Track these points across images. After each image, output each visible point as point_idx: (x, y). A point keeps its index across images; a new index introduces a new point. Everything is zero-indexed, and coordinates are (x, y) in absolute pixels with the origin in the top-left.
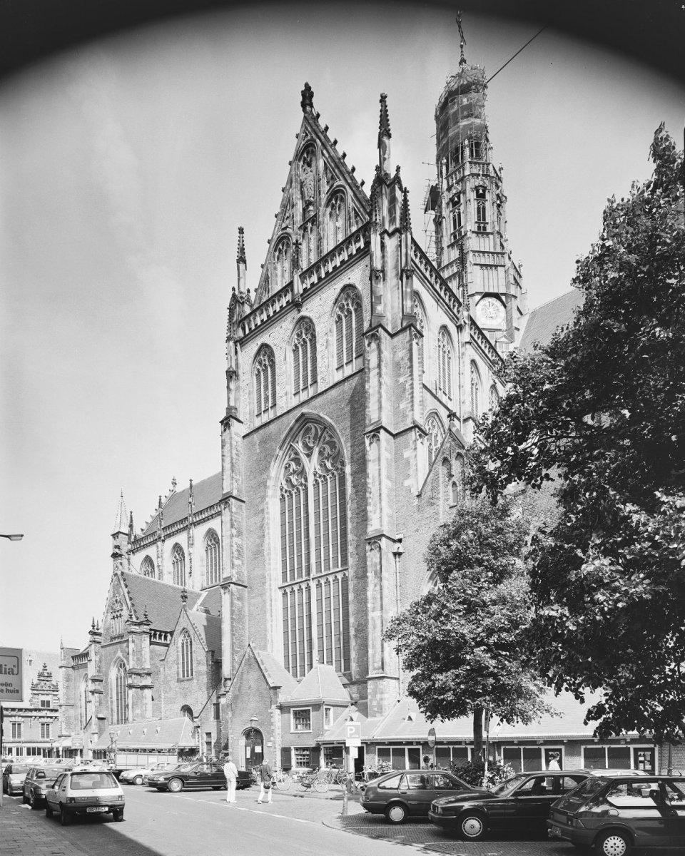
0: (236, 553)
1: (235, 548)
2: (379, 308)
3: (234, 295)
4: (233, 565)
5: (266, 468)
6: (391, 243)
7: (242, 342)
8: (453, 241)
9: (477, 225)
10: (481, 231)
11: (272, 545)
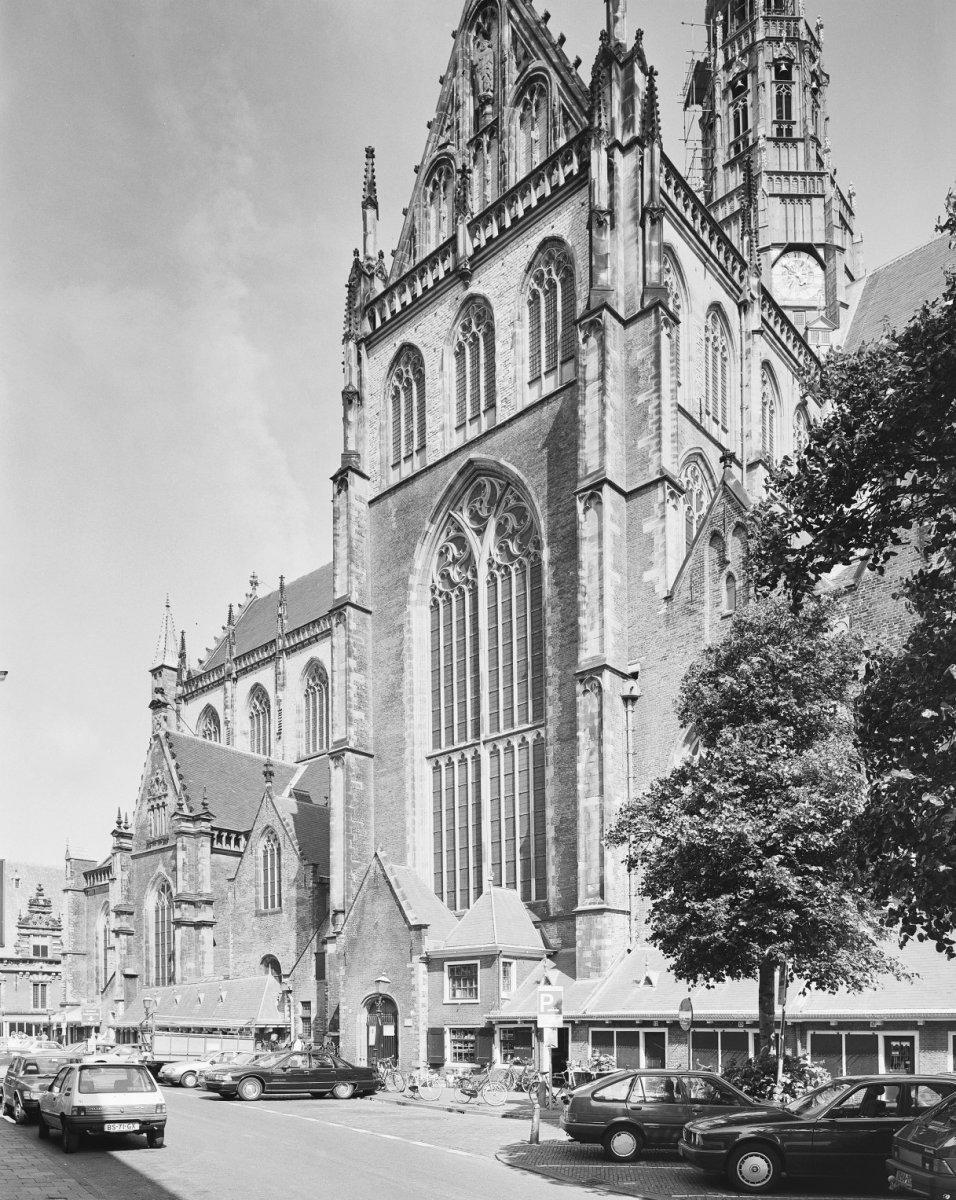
1: (353, 692)
2: (604, 277)
4: (349, 720)
5: (408, 555)
6: (625, 164)
8: (733, 156)
9: (776, 126)
10: (784, 137)
11: (416, 686)
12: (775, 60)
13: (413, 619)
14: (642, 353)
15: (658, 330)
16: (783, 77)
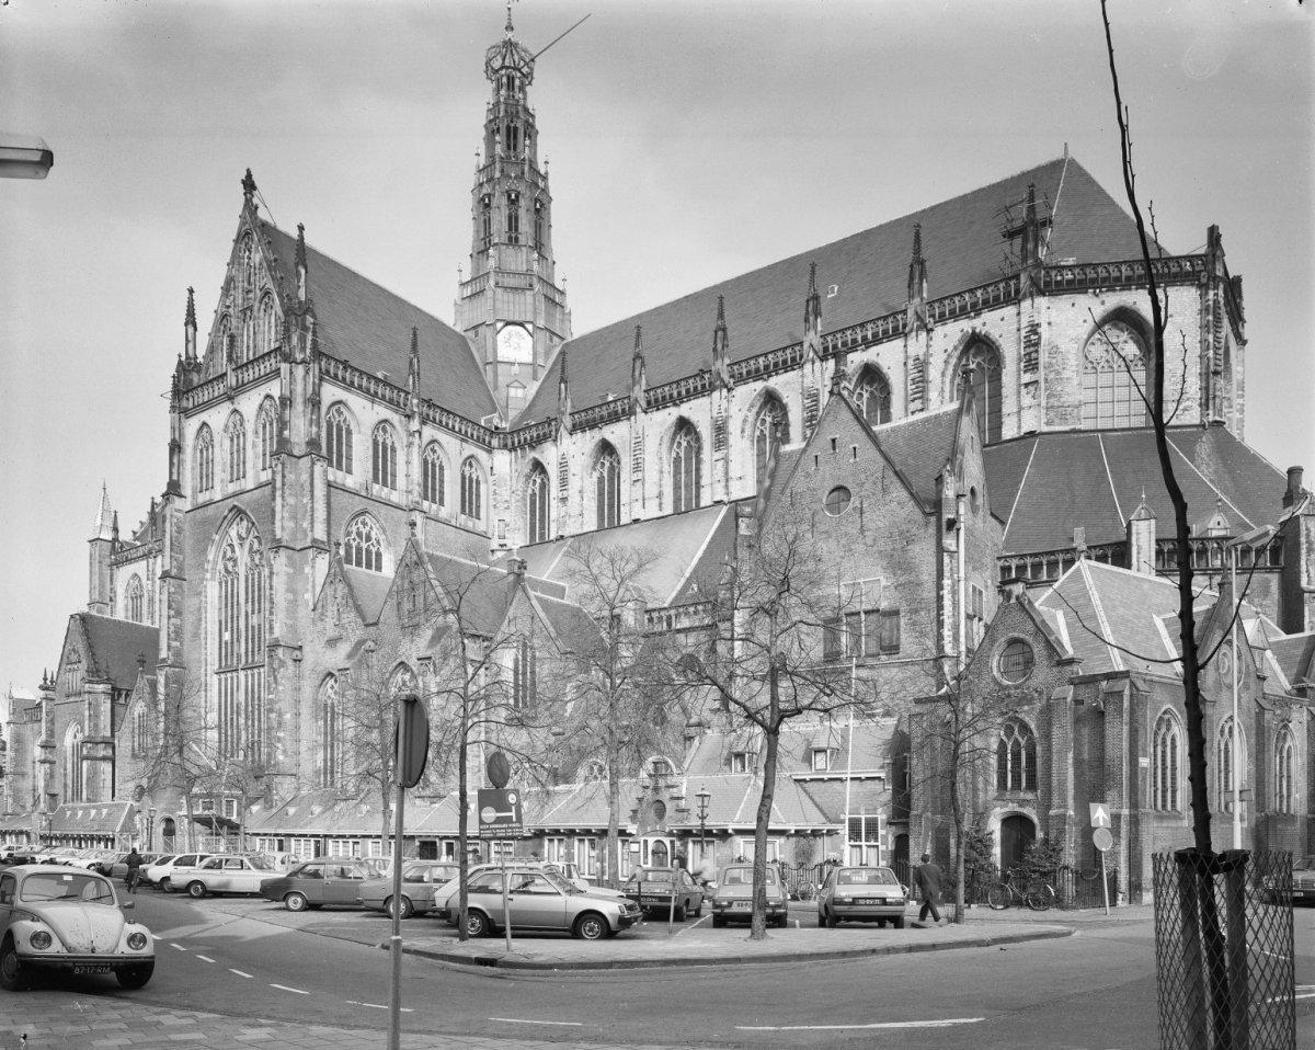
0: (172, 635)
1: (172, 628)
2: (286, 433)
3: (180, 362)
4: (169, 647)
5: (204, 551)
6: (300, 371)
7: (186, 413)
11: (209, 629)
12: (507, 192)
13: (209, 590)
14: (305, 477)
15: (313, 464)
16: (513, 202)
